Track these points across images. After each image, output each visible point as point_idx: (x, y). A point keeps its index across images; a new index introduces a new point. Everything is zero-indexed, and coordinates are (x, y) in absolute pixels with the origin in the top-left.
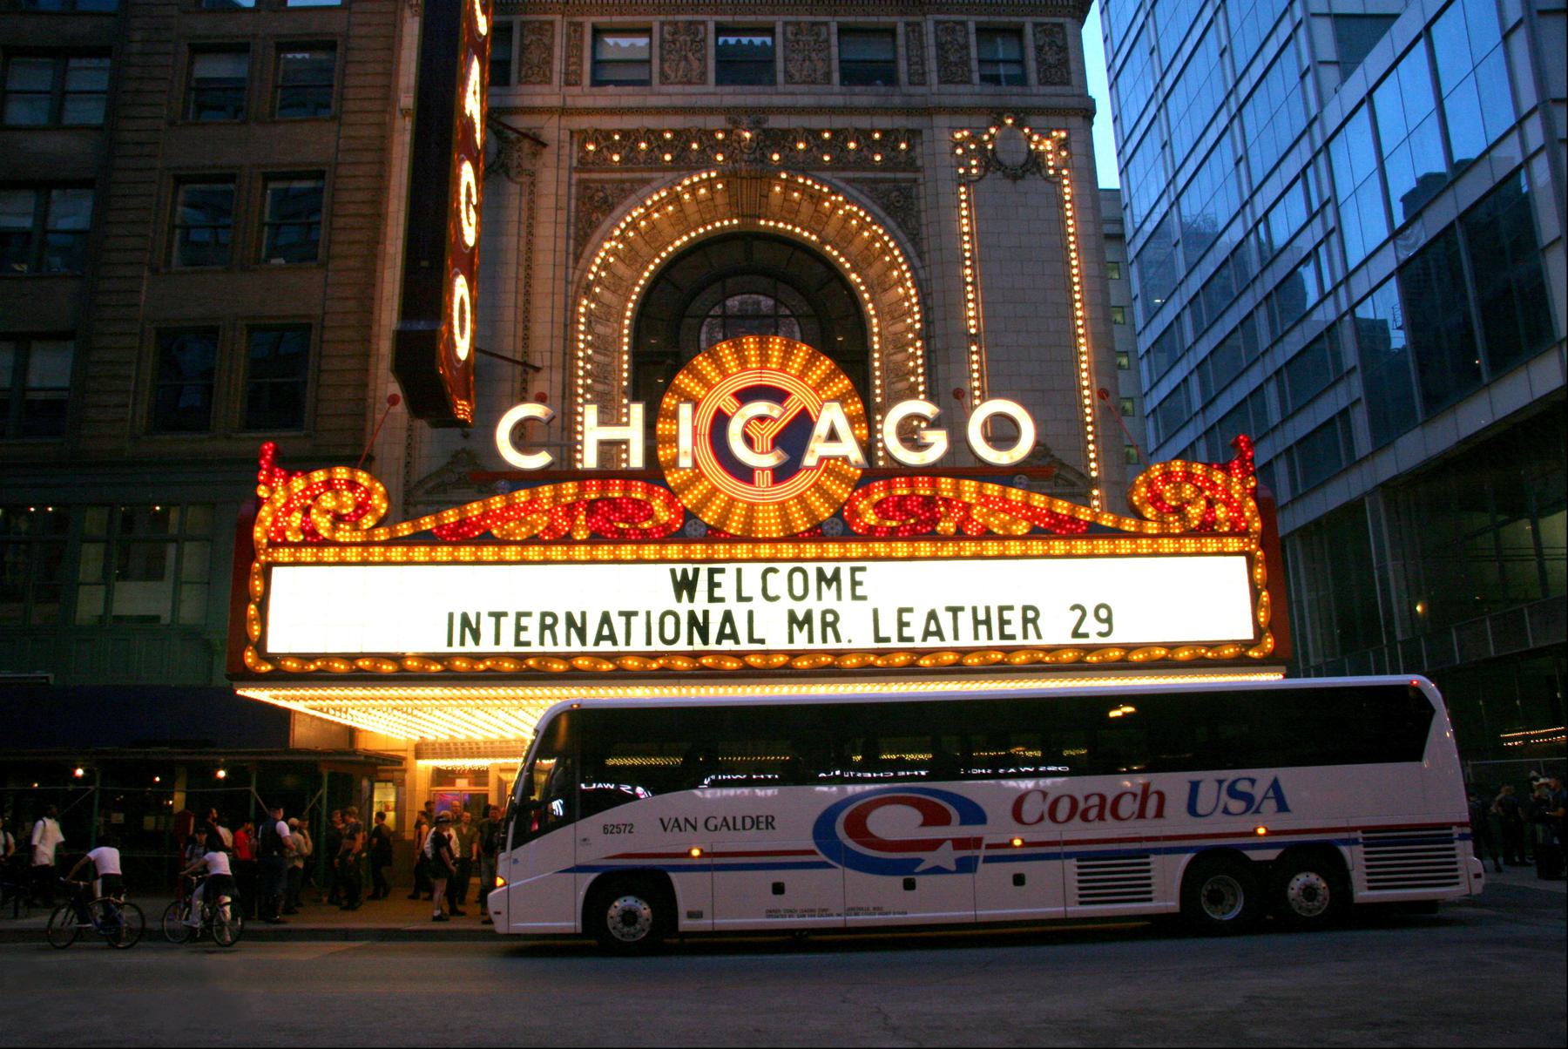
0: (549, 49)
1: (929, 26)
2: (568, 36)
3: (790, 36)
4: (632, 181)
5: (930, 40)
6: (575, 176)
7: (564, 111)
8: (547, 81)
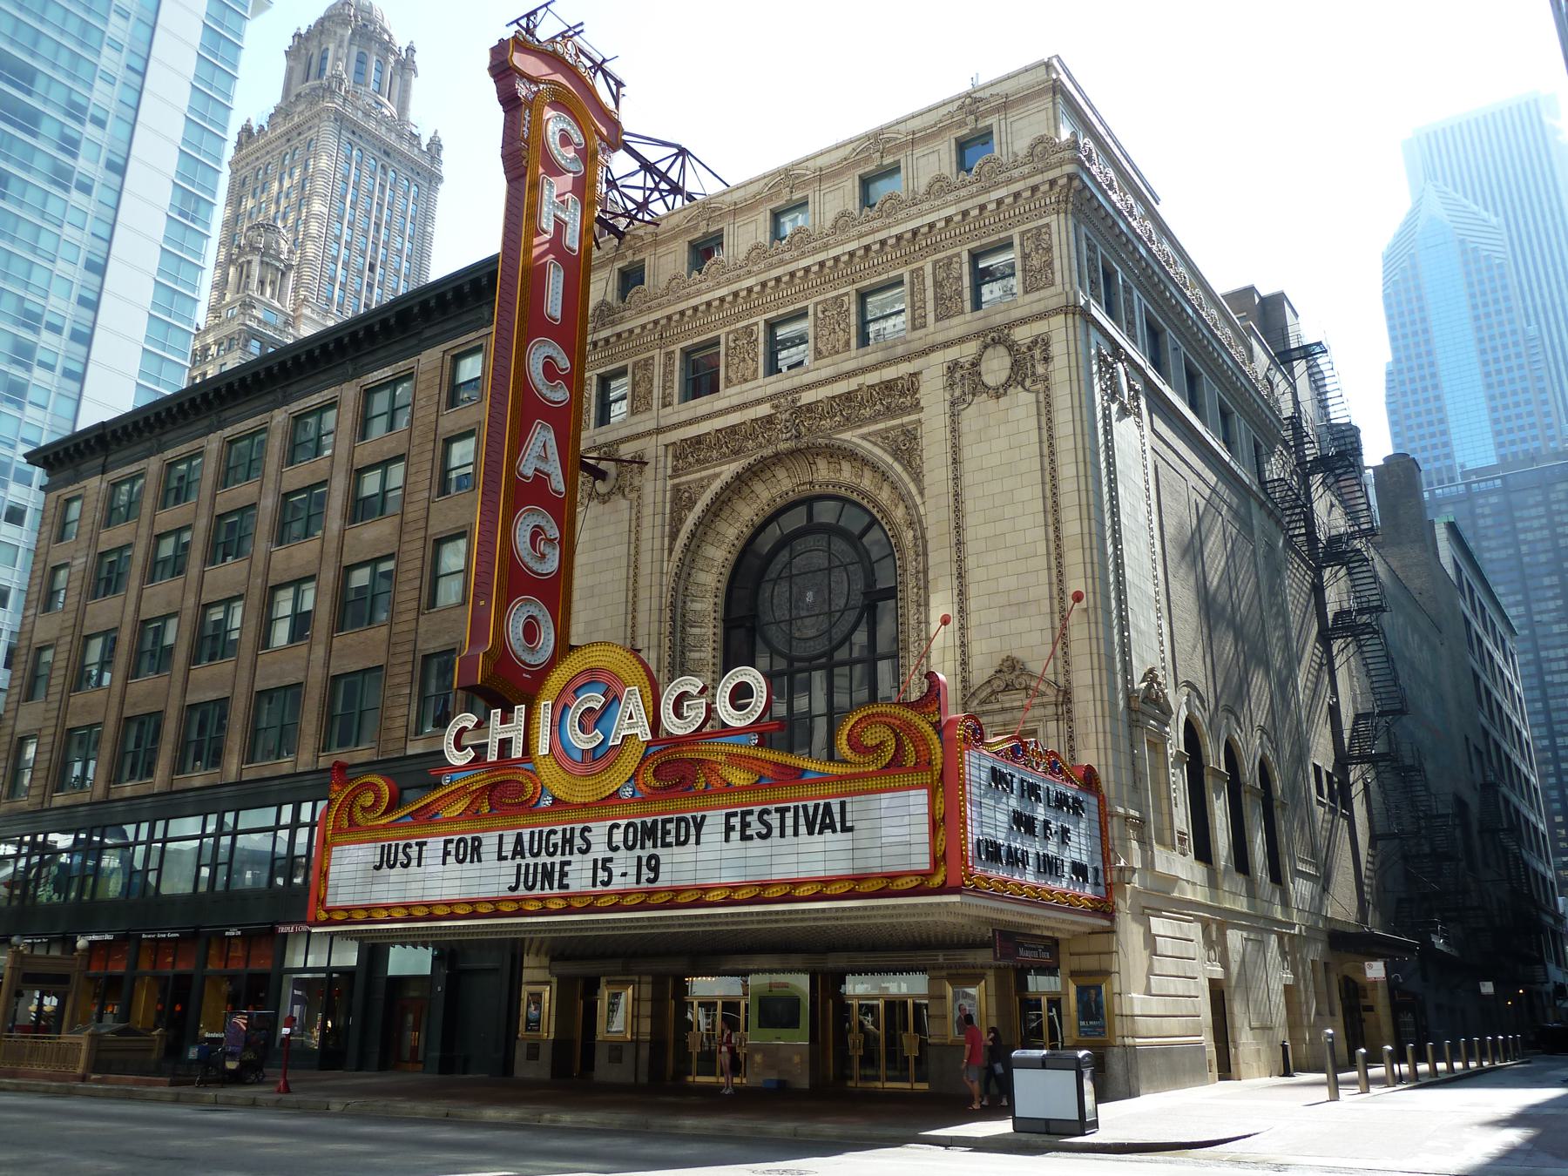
0: (651, 381)
1: (929, 269)
2: (665, 366)
3: (820, 315)
4: (708, 477)
5: (929, 282)
6: (670, 483)
7: (659, 431)
8: (649, 408)
